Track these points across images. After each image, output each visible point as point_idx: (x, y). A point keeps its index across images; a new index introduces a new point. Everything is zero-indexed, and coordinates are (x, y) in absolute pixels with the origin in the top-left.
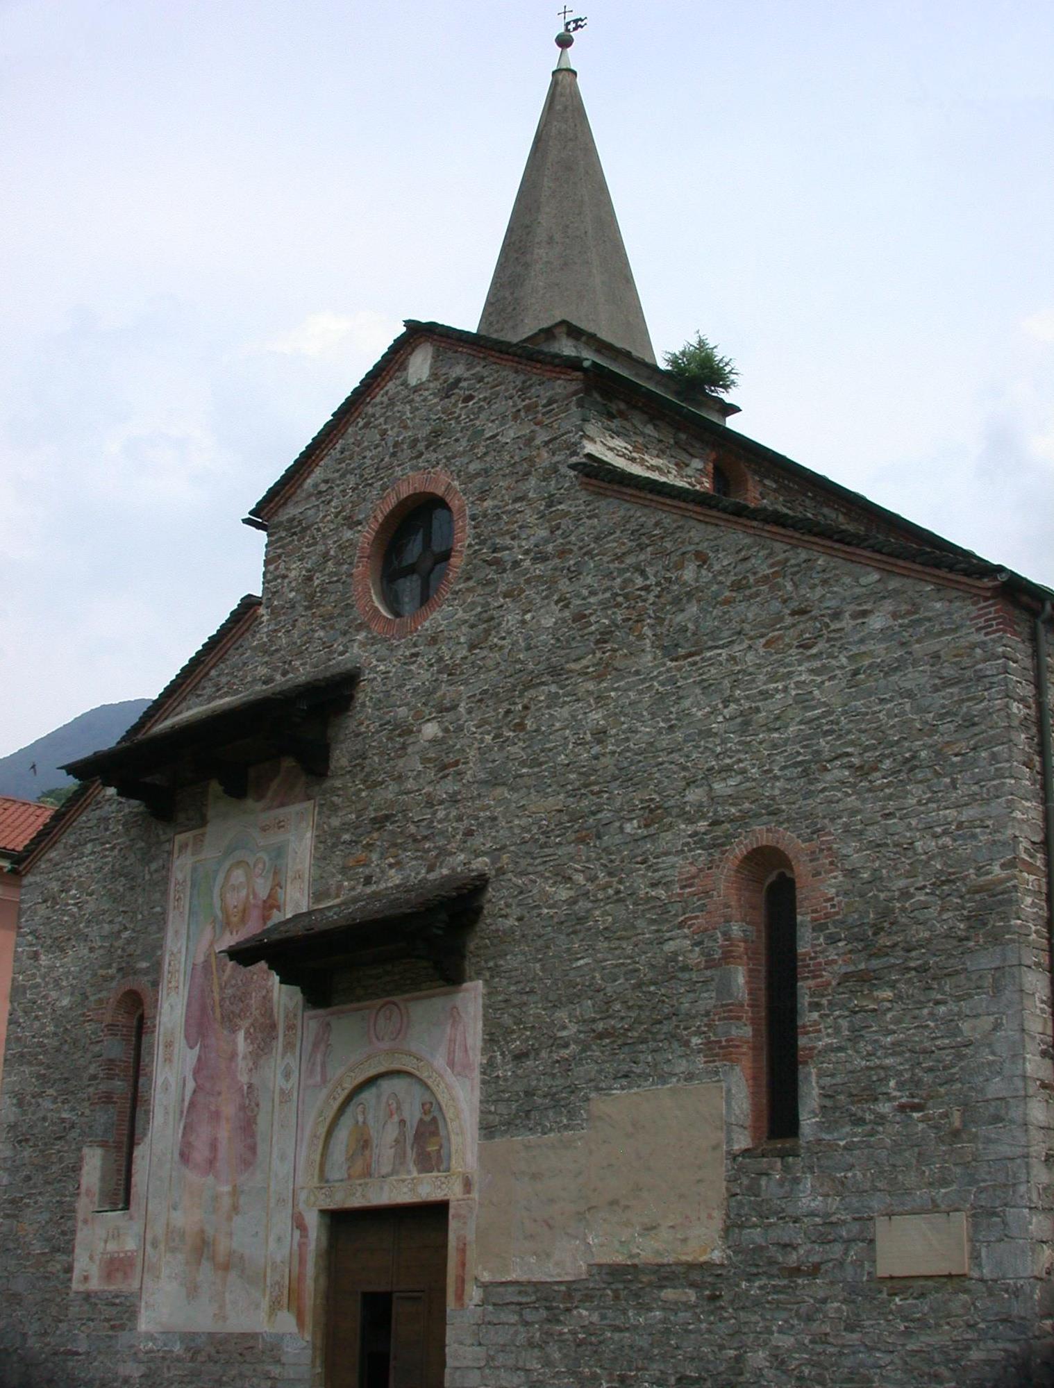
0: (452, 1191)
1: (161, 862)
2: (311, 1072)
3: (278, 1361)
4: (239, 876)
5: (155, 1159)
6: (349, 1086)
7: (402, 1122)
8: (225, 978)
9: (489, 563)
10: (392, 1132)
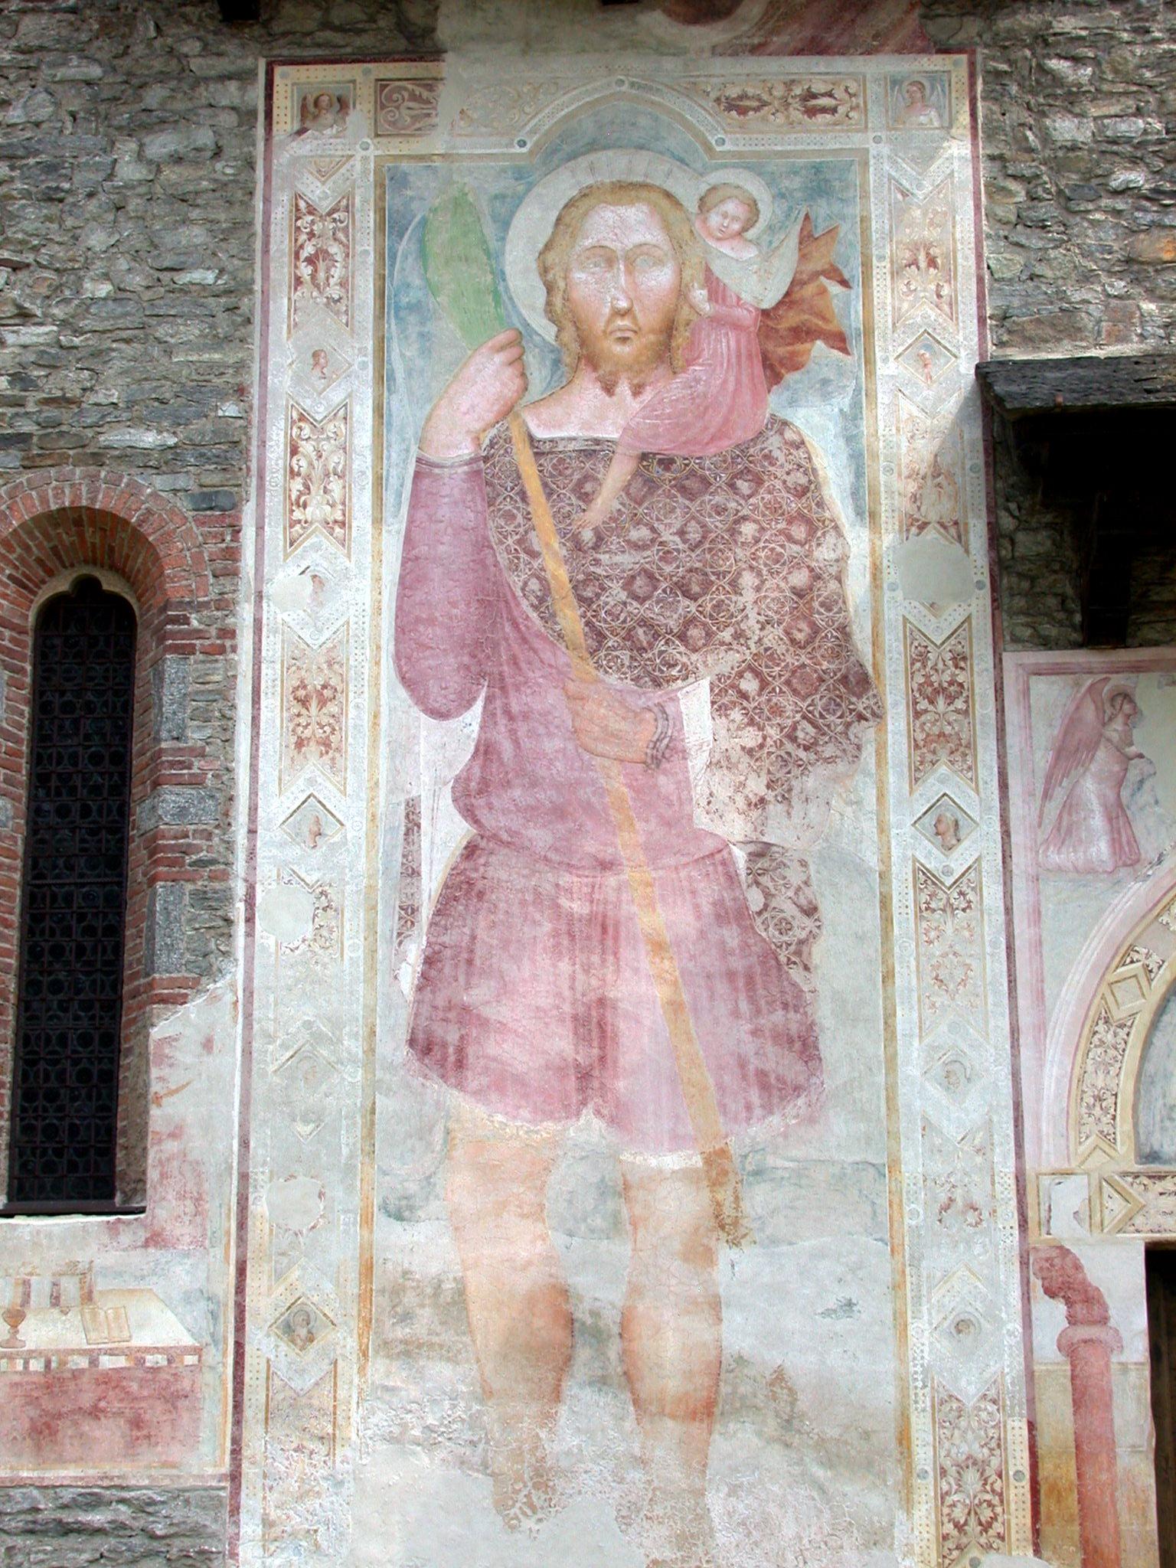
1: (205, 137)
2: (1065, 831)
4: (628, 224)
5: (272, 1057)
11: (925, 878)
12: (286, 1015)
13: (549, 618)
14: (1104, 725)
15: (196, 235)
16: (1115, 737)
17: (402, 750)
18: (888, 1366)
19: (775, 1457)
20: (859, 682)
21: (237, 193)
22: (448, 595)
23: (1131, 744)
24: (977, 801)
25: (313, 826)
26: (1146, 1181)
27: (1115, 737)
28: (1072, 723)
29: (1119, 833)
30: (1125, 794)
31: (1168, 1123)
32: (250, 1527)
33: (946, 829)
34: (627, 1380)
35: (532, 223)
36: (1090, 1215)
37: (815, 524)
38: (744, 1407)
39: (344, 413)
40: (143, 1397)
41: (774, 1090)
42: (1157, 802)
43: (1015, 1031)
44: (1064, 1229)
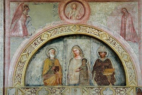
2: (15, 29)
14: (23, 11)
16: (25, 13)
23: (28, 15)
26: (26, 89)
27: (25, 13)
28: (17, 11)
29: (25, 30)
30: (26, 23)
31: (31, 80)
42: (31, 25)
43: (4, 64)
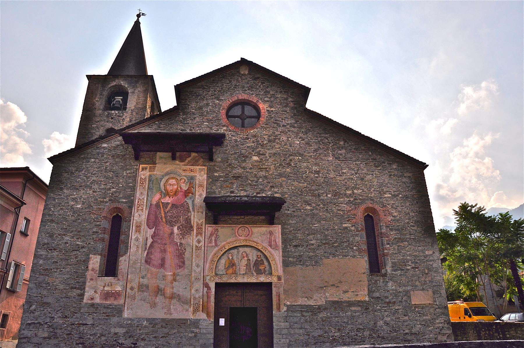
0: (274, 280)
1: (133, 171)
2: (210, 243)
3: (197, 327)
4: (173, 181)
5: (131, 262)
6: (227, 248)
7: (249, 260)
8: (167, 210)
9: (275, 123)
10: (244, 262)
11: (196, 246)
12: (133, 258)
13: (162, 220)
15: (131, 181)
17: (146, 232)
18: (189, 294)
19: (178, 303)
20: (192, 227)
21: (135, 177)
22: (152, 217)
24: (202, 239)
25: (137, 239)
32: (126, 308)
33: (199, 242)
34: (164, 295)
35: (164, 181)
36: (210, 280)
37: (189, 211)
38: (175, 298)
39: (143, 199)
40: (116, 295)
41: (180, 267)
44: (207, 281)
